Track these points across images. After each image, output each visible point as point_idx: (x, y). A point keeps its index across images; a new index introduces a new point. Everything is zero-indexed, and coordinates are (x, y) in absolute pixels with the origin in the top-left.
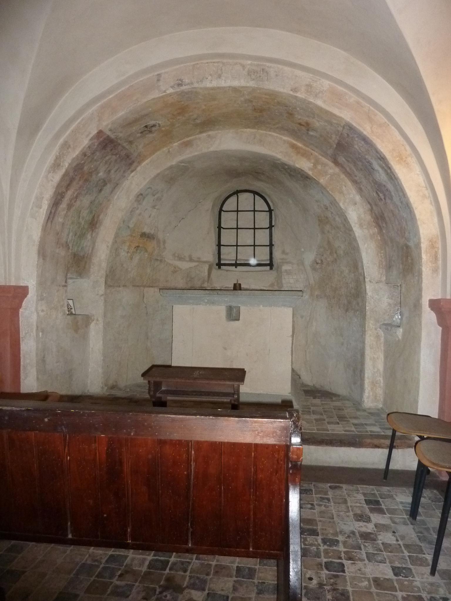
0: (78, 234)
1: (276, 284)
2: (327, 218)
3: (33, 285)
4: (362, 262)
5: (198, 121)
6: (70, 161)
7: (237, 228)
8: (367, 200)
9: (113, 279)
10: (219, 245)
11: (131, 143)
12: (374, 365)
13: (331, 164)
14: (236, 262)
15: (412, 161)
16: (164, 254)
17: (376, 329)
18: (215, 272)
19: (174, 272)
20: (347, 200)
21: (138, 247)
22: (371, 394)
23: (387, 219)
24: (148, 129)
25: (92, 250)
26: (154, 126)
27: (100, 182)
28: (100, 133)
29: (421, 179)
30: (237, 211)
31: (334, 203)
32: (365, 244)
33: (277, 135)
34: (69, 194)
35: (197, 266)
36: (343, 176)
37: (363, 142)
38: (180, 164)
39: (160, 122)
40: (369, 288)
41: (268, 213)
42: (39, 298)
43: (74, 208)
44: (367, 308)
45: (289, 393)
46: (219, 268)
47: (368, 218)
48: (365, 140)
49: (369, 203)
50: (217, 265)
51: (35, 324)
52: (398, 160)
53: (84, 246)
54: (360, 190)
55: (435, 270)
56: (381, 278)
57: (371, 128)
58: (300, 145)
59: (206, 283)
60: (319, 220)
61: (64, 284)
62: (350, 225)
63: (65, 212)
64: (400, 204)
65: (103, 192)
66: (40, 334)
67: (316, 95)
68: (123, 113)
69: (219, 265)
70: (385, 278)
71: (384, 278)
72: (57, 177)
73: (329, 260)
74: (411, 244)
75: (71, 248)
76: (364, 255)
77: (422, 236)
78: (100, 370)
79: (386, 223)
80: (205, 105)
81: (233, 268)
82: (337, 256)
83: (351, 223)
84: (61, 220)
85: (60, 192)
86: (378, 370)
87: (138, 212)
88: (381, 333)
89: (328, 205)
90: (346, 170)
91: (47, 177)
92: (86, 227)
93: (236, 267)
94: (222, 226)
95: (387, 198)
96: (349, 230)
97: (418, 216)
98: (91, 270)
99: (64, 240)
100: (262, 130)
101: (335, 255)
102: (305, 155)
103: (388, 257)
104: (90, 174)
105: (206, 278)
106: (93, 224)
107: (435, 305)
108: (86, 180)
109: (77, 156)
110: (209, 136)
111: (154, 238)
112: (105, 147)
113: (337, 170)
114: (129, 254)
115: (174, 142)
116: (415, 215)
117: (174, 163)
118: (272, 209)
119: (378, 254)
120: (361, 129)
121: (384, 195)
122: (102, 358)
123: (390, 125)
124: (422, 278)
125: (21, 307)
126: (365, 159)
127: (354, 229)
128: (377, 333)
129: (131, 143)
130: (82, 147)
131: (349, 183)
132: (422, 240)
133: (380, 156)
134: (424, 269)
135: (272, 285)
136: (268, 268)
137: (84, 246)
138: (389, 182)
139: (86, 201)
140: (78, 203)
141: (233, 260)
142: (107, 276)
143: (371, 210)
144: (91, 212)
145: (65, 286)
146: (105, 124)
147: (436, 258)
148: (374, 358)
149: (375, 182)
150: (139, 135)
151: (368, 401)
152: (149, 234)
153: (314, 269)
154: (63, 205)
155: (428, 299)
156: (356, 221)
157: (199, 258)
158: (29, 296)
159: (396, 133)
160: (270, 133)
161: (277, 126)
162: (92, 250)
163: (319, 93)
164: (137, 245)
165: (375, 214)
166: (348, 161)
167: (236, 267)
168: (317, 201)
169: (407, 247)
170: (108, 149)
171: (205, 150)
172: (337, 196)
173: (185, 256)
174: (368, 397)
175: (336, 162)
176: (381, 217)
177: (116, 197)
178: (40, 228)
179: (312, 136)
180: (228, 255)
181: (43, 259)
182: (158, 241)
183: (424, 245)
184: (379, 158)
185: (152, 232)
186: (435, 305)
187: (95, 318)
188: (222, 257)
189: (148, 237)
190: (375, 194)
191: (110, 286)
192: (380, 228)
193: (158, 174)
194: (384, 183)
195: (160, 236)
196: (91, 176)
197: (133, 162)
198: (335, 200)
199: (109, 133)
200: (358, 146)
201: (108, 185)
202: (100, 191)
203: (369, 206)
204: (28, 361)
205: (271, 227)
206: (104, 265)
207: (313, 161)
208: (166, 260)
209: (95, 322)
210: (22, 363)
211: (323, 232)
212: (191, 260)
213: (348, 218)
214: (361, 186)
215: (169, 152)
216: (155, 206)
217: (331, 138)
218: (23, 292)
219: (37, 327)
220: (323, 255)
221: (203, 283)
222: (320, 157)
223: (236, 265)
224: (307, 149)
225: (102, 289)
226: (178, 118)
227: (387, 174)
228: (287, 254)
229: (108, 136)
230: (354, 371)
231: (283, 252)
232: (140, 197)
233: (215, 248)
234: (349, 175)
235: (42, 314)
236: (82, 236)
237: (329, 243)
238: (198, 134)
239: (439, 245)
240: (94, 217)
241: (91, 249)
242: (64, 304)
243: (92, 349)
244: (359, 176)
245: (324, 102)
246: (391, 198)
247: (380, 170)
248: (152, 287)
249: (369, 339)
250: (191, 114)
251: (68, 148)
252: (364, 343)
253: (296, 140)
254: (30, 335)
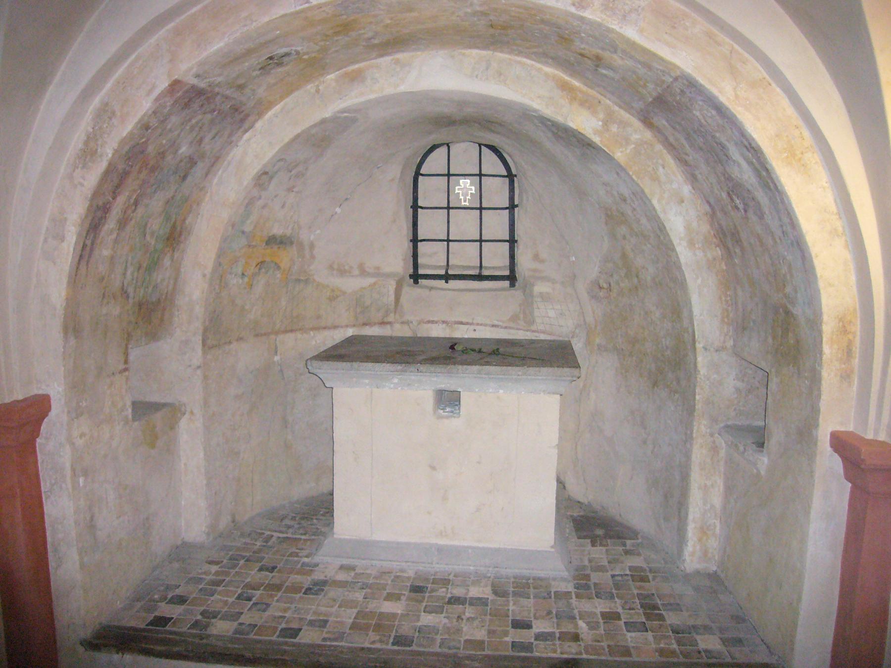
0: (145, 265)
1: (521, 316)
2: (622, 214)
3: (58, 392)
4: (691, 312)
5: (376, 41)
6: (115, 145)
7: (448, 208)
8: (705, 197)
9: (216, 333)
10: (415, 241)
11: (241, 87)
12: (706, 497)
13: (636, 123)
14: (447, 272)
15: (814, 159)
16: (312, 268)
17: (712, 435)
18: (410, 292)
19: (332, 299)
20: (666, 195)
21: (262, 262)
22: (698, 547)
23: (745, 244)
24: (275, 61)
25: (175, 284)
26: (287, 54)
27: (183, 164)
28: (175, 85)
29: (828, 198)
30: (449, 175)
31: (640, 196)
32: (697, 278)
33: (533, 63)
34: (121, 199)
35: (375, 284)
36: (659, 147)
37: (714, 112)
38: (339, 115)
39: (299, 49)
40: (702, 360)
41: (507, 180)
42: (74, 415)
43: (133, 222)
44: (697, 397)
45: (552, 547)
46: (416, 282)
47: (705, 228)
48: (720, 109)
49: (708, 202)
50: (411, 276)
51: (68, 465)
52: (787, 157)
53: (159, 280)
54: (693, 179)
55: (846, 376)
56: (724, 342)
57: (735, 89)
58: (576, 83)
59: (392, 315)
60: (607, 215)
61: (122, 366)
62: (671, 241)
63: (114, 236)
64: (781, 235)
65: (189, 179)
66: (81, 480)
67: (624, 17)
68: (222, 44)
69: (416, 277)
70: (731, 343)
71: (731, 343)
72: (92, 178)
73: (622, 285)
74: (797, 311)
75: (131, 295)
76: (695, 299)
77: (825, 309)
78: (203, 503)
79: (743, 249)
80: (391, 19)
81: (441, 283)
82: (639, 282)
83: (673, 238)
84: (106, 253)
85: (101, 203)
86: (712, 506)
87: (260, 203)
88: (721, 442)
89: (627, 196)
90: (666, 138)
91: (70, 177)
92: (160, 246)
93: (447, 282)
94: (420, 203)
95: (751, 214)
96: (665, 246)
97: (819, 271)
98: (176, 319)
99: (118, 284)
100: (502, 52)
101: (635, 280)
102: (587, 104)
103: (740, 306)
104: (162, 155)
105: (392, 307)
106: (174, 237)
107: (839, 443)
108: (153, 170)
109: (131, 133)
110: (397, 62)
111: (292, 243)
112: (187, 105)
113: (648, 135)
114: (246, 279)
115: (329, 74)
116: (813, 268)
117: (327, 114)
118: (514, 172)
119: (720, 298)
120: (715, 91)
121: (746, 205)
122: (205, 482)
123: (774, 85)
124: (819, 389)
125: (38, 436)
126: (713, 137)
127: (679, 249)
128: (714, 442)
129: (241, 87)
130: (139, 116)
131: (670, 160)
132: (825, 318)
133: (750, 144)
134: (825, 374)
135: (514, 318)
136: (507, 283)
137: (159, 280)
138: (760, 190)
139: (156, 203)
140: (140, 210)
141: (440, 267)
142: (206, 330)
143: (713, 215)
144: (168, 219)
145: (126, 370)
146: (184, 67)
147: (849, 353)
148: (706, 486)
149: (729, 178)
150: (258, 73)
151: (692, 561)
152: (281, 237)
153: (594, 297)
154: (111, 224)
155: (830, 430)
156: (682, 235)
157: (378, 268)
158: (53, 413)
159: (785, 102)
160: (519, 59)
161: (535, 50)
162: (175, 284)
163: (631, 11)
164: (260, 260)
165: (719, 225)
166: (674, 128)
167: (447, 282)
168: (605, 184)
169: (788, 313)
170: (195, 106)
171: (389, 91)
172: (647, 186)
173: (351, 267)
174: (692, 554)
175: (647, 122)
176: (733, 234)
177: (215, 181)
178: (65, 280)
179: (605, 76)
180: (432, 257)
181: (76, 337)
182: (301, 246)
183: (828, 327)
184: (746, 147)
185: (288, 232)
186: (839, 443)
187: (188, 410)
188: (420, 261)
189: (281, 243)
190: (724, 195)
191: (211, 348)
192: (729, 255)
193: (298, 136)
194: (750, 188)
195: (305, 236)
196: (163, 158)
197: (247, 116)
198: (643, 191)
199: (195, 81)
200: (700, 112)
201: (200, 165)
202: (184, 178)
203: (707, 207)
204: (61, 536)
205: (512, 207)
206: (199, 310)
207: (601, 116)
208: (316, 277)
209: (187, 416)
210: (49, 539)
211: (613, 236)
212: (363, 272)
213: (668, 228)
214: (697, 173)
215: (318, 91)
216: (294, 187)
217: (645, 86)
218: (39, 406)
219: (73, 470)
220: (612, 276)
221: (387, 313)
222: (617, 108)
223: (447, 277)
224: (590, 91)
225: (197, 356)
226: (336, 38)
227: (759, 175)
228: (542, 261)
229: (193, 87)
230: (666, 496)
231: (536, 257)
232: (264, 177)
233: (407, 246)
234: (671, 147)
235: (80, 442)
236: (154, 265)
237: (624, 256)
238: (375, 58)
239: (857, 328)
240: (174, 227)
241: (172, 282)
242: (125, 405)
243: (185, 464)
244: (693, 156)
245: (641, 31)
246: (761, 217)
247: (744, 164)
248: (292, 331)
249: (699, 454)
250: (363, 31)
251: (110, 118)
252: (688, 455)
253: (571, 75)
254: (61, 487)
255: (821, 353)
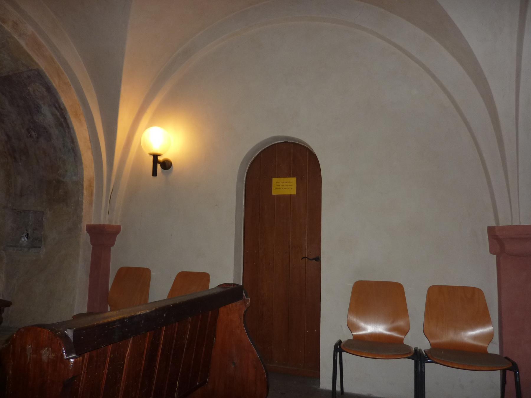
15: (83, 118)
37: (44, 90)
77: (85, 176)
120: (52, 81)
133: (59, 106)
134: (84, 201)
183: (86, 184)
255: (83, 193)
